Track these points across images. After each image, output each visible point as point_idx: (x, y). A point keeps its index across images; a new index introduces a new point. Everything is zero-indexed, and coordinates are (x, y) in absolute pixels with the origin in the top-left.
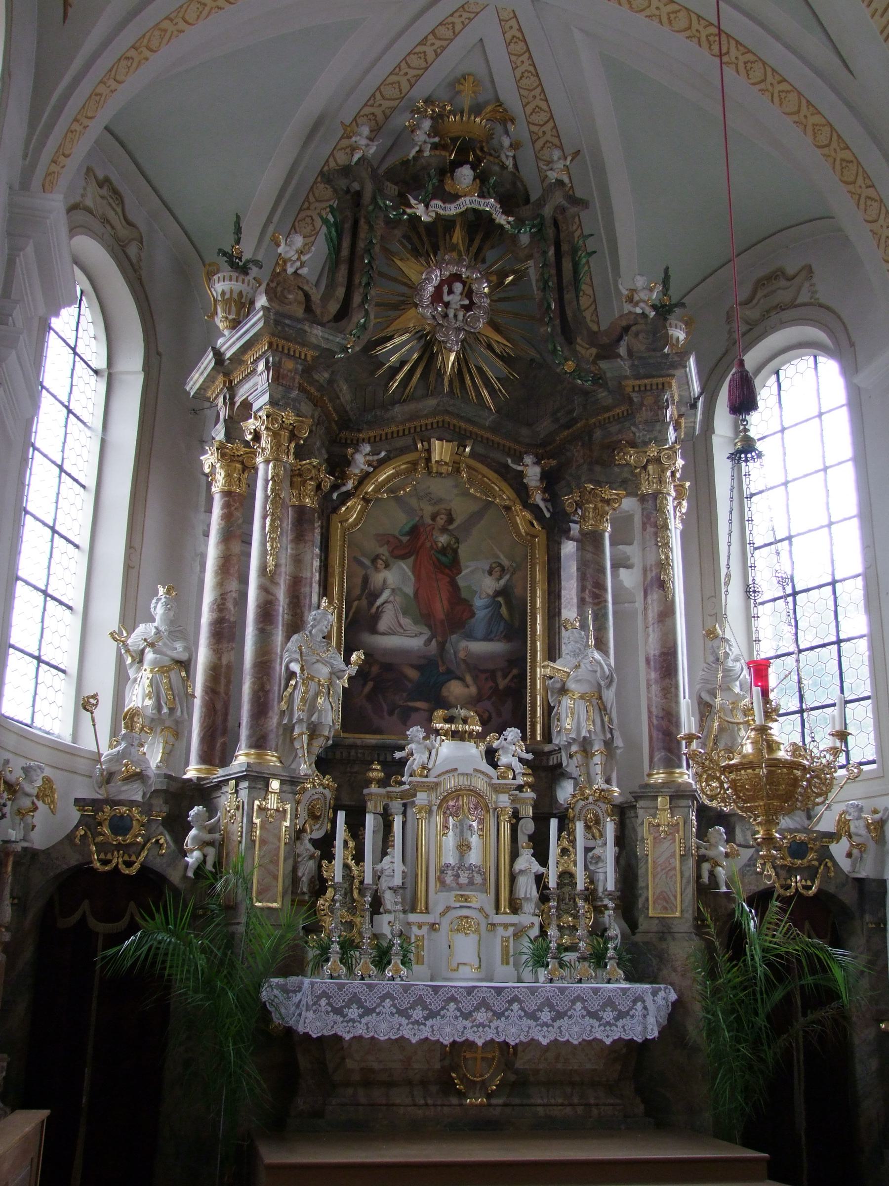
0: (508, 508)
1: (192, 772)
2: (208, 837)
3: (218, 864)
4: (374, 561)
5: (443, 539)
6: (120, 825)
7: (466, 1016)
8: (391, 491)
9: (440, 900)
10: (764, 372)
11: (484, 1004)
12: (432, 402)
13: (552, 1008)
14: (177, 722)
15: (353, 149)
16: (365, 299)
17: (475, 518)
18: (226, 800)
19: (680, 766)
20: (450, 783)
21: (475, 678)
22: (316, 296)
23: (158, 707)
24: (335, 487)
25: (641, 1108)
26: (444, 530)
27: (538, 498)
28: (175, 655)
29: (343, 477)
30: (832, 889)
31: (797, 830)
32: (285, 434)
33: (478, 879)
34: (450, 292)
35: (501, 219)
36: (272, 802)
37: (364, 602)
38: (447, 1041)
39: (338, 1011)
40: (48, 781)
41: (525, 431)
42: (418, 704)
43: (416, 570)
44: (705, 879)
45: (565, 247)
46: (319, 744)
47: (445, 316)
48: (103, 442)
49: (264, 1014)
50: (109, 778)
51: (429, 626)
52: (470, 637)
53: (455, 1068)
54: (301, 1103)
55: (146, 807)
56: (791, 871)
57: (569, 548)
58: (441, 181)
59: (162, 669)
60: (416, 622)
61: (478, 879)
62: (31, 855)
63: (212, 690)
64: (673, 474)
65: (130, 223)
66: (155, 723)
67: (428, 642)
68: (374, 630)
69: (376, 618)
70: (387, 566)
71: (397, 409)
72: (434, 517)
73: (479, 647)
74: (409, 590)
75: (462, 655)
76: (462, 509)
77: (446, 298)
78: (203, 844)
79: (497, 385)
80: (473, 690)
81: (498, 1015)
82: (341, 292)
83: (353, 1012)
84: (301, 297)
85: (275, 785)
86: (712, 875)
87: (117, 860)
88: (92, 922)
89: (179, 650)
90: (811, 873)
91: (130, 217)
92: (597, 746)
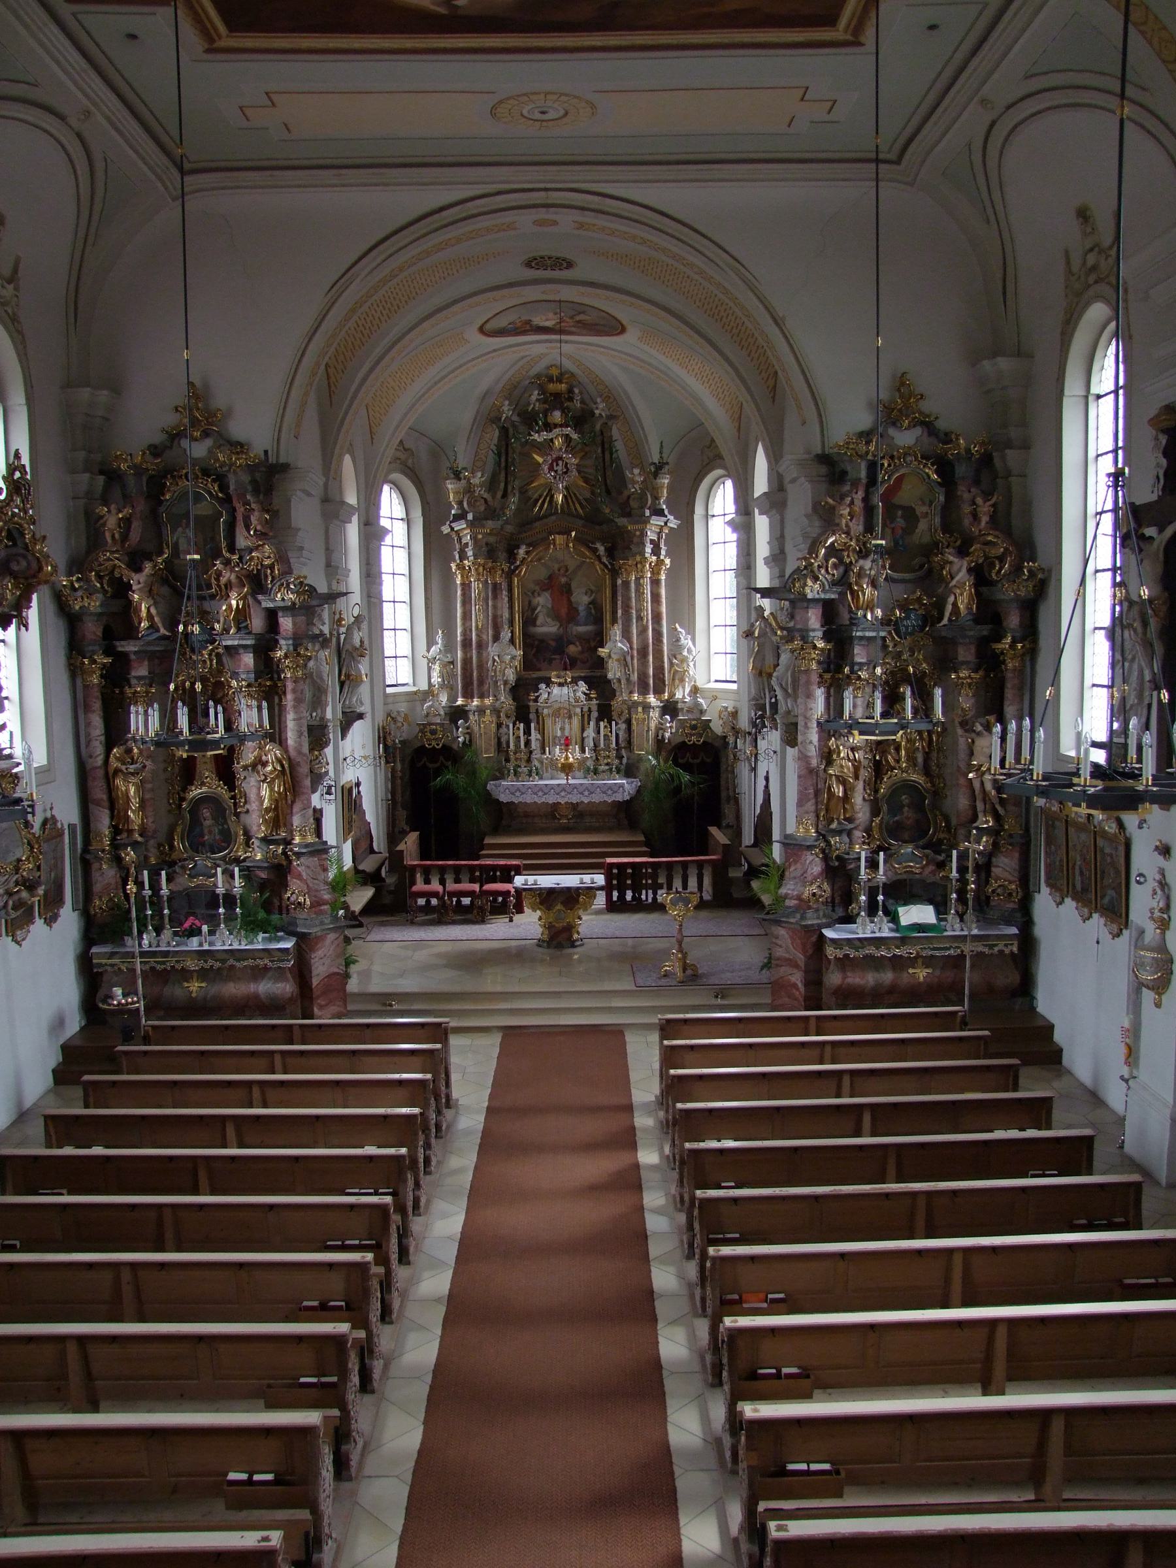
1: (460, 702)
3: (470, 741)
4: (533, 593)
5: (563, 580)
6: (433, 732)
12: (554, 518)
17: (579, 567)
19: (649, 694)
20: (556, 706)
21: (581, 643)
23: (443, 681)
24: (510, 567)
25: (626, 822)
26: (564, 575)
27: (604, 560)
28: (447, 660)
29: (515, 559)
30: (710, 741)
31: (694, 720)
32: (481, 569)
34: (557, 465)
35: (575, 436)
37: (530, 613)
39: (513, 794)
41: (597, 527)
43: (551, 595)
44: (660, 738)
45: (606, 446)
46: (509, 686)
48: (409, 554)
50: (427, 715)
52: (578, 624)
53: (556, 810)
54: (504, 822)
56: (691, 735)
57: (619, 582)
58: (546, 416)
59: (444, 665)
63: (464, 669)
65: (405, 450)
66: (442, 686)
68: (535, 625)
69: (535, 619)
70: (539, 595)
71: (537, 524)
72: (559, 570)
73: (581, 629)
74: (550, 606)
75: (575, 633)
76: (572, 565)
78: (464, 734)
80: (580, 648)
84: (483, 501)
86: (663, 736)
87: (434, 743)
88: (428, 764)
89: (449, 658)
91: (406, 447)
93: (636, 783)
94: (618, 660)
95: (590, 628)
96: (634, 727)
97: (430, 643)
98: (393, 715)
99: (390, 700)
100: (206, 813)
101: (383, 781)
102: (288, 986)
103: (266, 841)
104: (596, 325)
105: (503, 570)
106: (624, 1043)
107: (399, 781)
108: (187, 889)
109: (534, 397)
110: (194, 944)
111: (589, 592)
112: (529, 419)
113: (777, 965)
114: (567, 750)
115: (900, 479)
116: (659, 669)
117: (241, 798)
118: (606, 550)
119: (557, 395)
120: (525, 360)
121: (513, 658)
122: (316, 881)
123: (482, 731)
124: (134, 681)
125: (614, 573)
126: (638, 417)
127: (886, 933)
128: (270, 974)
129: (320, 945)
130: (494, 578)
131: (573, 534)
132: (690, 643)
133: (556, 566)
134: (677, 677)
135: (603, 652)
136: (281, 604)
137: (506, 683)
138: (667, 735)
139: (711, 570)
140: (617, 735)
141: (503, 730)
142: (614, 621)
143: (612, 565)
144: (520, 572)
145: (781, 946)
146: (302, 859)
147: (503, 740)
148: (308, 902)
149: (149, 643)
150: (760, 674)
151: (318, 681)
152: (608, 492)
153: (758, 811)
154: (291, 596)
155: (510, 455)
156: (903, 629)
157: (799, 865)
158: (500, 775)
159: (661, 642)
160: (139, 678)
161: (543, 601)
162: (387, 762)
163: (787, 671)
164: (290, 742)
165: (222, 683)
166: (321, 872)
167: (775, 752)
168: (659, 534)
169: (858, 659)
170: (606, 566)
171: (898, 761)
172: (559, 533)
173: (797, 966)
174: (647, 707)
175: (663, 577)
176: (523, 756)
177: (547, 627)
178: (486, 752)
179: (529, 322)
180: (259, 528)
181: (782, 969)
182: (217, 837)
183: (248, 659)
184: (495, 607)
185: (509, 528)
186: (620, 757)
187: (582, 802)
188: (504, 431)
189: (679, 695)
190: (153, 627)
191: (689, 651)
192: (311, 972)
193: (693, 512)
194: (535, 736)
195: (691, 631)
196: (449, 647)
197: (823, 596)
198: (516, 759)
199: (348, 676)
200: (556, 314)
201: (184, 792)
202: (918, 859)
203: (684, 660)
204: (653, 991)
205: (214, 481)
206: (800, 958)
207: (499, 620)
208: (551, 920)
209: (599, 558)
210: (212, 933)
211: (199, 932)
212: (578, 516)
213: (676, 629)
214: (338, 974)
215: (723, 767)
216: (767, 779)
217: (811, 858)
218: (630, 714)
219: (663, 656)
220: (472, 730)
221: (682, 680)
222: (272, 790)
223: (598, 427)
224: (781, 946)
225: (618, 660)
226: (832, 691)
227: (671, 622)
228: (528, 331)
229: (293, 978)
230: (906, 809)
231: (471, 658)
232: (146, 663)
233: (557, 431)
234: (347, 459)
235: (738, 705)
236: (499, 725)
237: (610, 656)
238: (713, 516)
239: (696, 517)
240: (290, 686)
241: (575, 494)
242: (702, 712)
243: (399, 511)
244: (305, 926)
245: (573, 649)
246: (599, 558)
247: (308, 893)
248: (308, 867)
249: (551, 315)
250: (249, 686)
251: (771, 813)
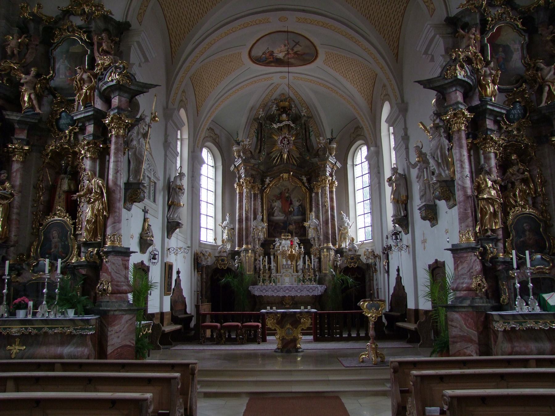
0: (301, 187)
1: (236, 249)
2: (239, 261)
4: (273, 201)
5: (287, 195)
6: (223, 260)
7: (285, 291)
8: (276, 185)
9: (282, 271)
10: (358, 149)
11: (288, 289)
12: (282, 165)
13: (300, 289)
14: (233, 240)
15: (260, 114)
16: (264, 148)
18: (242, 255)
21: (295, 224)
22: (253, 151)
23: (229, 237)
24: (262, 187)
26: (287, 193)
27: (306, 184)
29: (265, 184)
30: (360, 266)
32: (248, 182)
33: (290, 267)
34: (284, 141)
35: (292, 125)
36: (249, 255)
37: (271, 210)
38: (281, 296)
39: (261, 291)
40: (210, 253)
42: (283, 231)
44: (335, 265)
45: (307, 129)
46: (261, 242)
47: (283, 146)
49: (249, 292)
50: (220, 252)
51: (285, 214)
52: (294, 215)
55: (227, 257)
56: (351, 263)
57: (313, 195)
58: (279, 118)
59: (229, 230)
60: (282, 213)
61: (290, 267)
62: (208, 267)
63: (239, 233)
64: (329, 181)
65: (215, 134)
66: (228, 240)
67: (285, 217)
68: (273, 216)
69: (274, 213)
70: (275, 202)
72: (285, 190)
74: (280, 207)
77: (283, 142)
79: (297, 159)
80: (295, 227)
81: (290, 291)
82: (259, 147)
83: (264, 291)
85: (250, 251)
86: (337, 264)
87: (223, 266)
89: (232, 226)
90: (355, 263)
91: (216, 133)
92: (316, 239)
93: (324, 287)
94: (313, 229)
95: (300, 217)
96: (322, 259)
97: (224, 219)
98: (203, 253)
99: (202, 246)
100: (55, 234)
101: (196, 281)
102: (86, 350)
103: (87, 244)
104: (304, 54)
105: (259, 188)
106: (342, 404)
107: (204, 284)
108: (30, 281)
109: (274, 108)
110: (21, 314)
111: (299, 200)
112: (271, 119)
113: (454, 342)
114: (291, 248)
115: (499, 29)
116: (334, 233)
117: (79, 224)
118: (307, 179)
119: (284, 108)
120: (271, 88)
121: (263, 228)
122: (118, 275)
123: (247, 261)
124: (15, 141)
125: (311, 190)
126: (321, 120)
127: (538, 310)
128: (75, 341)
129: (116, 322)
130: (255, 191)
131: (292, 173)
132: (348, 220)
133: (284, 188)
134: (342, 237)
135: (306, 224)
136: (111, 84)
137: (259, 240)
138: (338, 263)
139: (356, 189)
140: (314, 265)
141: (257, 262)
142: (311, 210)
143: (310, 187)
144: (267, 191)
145: (456, 327)
146: (109, 257)
147: (257, 267)
148: (110, 288)
149: (27, 116)
150: (398, 202)
151: (139, 156)
152: (308, 150)
153: (392, 291)
154: (117, 77)
155: (263, 134)
156: (511, 116)
157: (465, 265)
158: (255, 283)
159: (334, 220)
160: (17, 139)
161: (277, 204)
162: (198, 271)
163: (437, 149)
164: (111, 177)
165: (76, 152)
166: (123, 269)
167: (407, 246)
168: (332, 169)
169: (489, 127)
170: (307, 188)
171: (516, 202)
172: (285, 173)
173: (471, 341)
174: (329, 249)
175: (334, 190)
176: (267, 276)
177: (279, 217)
178: (249, 272)
179: (272, 53)
180: (105, 48)
181: (458, 345)
182: (60, 250)
183: (90, 129)
184: (255, 204)
185: (262, 168)
186: (316, 276)
187: (297, 296)
188: (260, 125)
189: (343, 245)
190: (32, 107)
191: (348, 224)
192: (107, 341)
193: (347, 163)
194: (273, 264)
195: (348, 215)
196: (232, 221)
197: (466, 79)
198: (264, 276)
199: (172, 202)
200: (285, 46)
201: (43, 220)
202: (546, 263)
203: (346, 228)
204: (357, 370)
205: (84, 32)
206: (474, 334)
207: (257, 210)
208: (284, 334)
209: (303, 183)
210: (36, 307)
211: (25, 307)
212: (294, 165)
213: (342, 214)
214: (130, 346)
215: (367, 280)
216: (398, 270)
217: (474, 258)
218: (320, 254)
219: (335, 227)
220: (242, 261)
221: (345, 239)
222: (93, 209)
223: (303, 121)
224: (456, 327)
225: (313, 229)
226: (472, 152)
227: (339, 214)
228: (271, 62)
229: (94, 346)
230: (527, 233)
231: (243, 228)
232: (26, 132)
233: (284, 123)
234: (182, 112)
235: (374, 248)
236: (255, 260)
237: (309, 227)
238: (356, 165)
239: (348, 166)
240: (113, 140)
241: (293, 156)
242: (355, 251)
243: (211, 162)
244: (106, 306)
245: (291, 227)
246: (303, 183)
247: (111, 282)
248: (114, 264)
249: (283, 48)
250: (88, 144)
251: (404, 287)
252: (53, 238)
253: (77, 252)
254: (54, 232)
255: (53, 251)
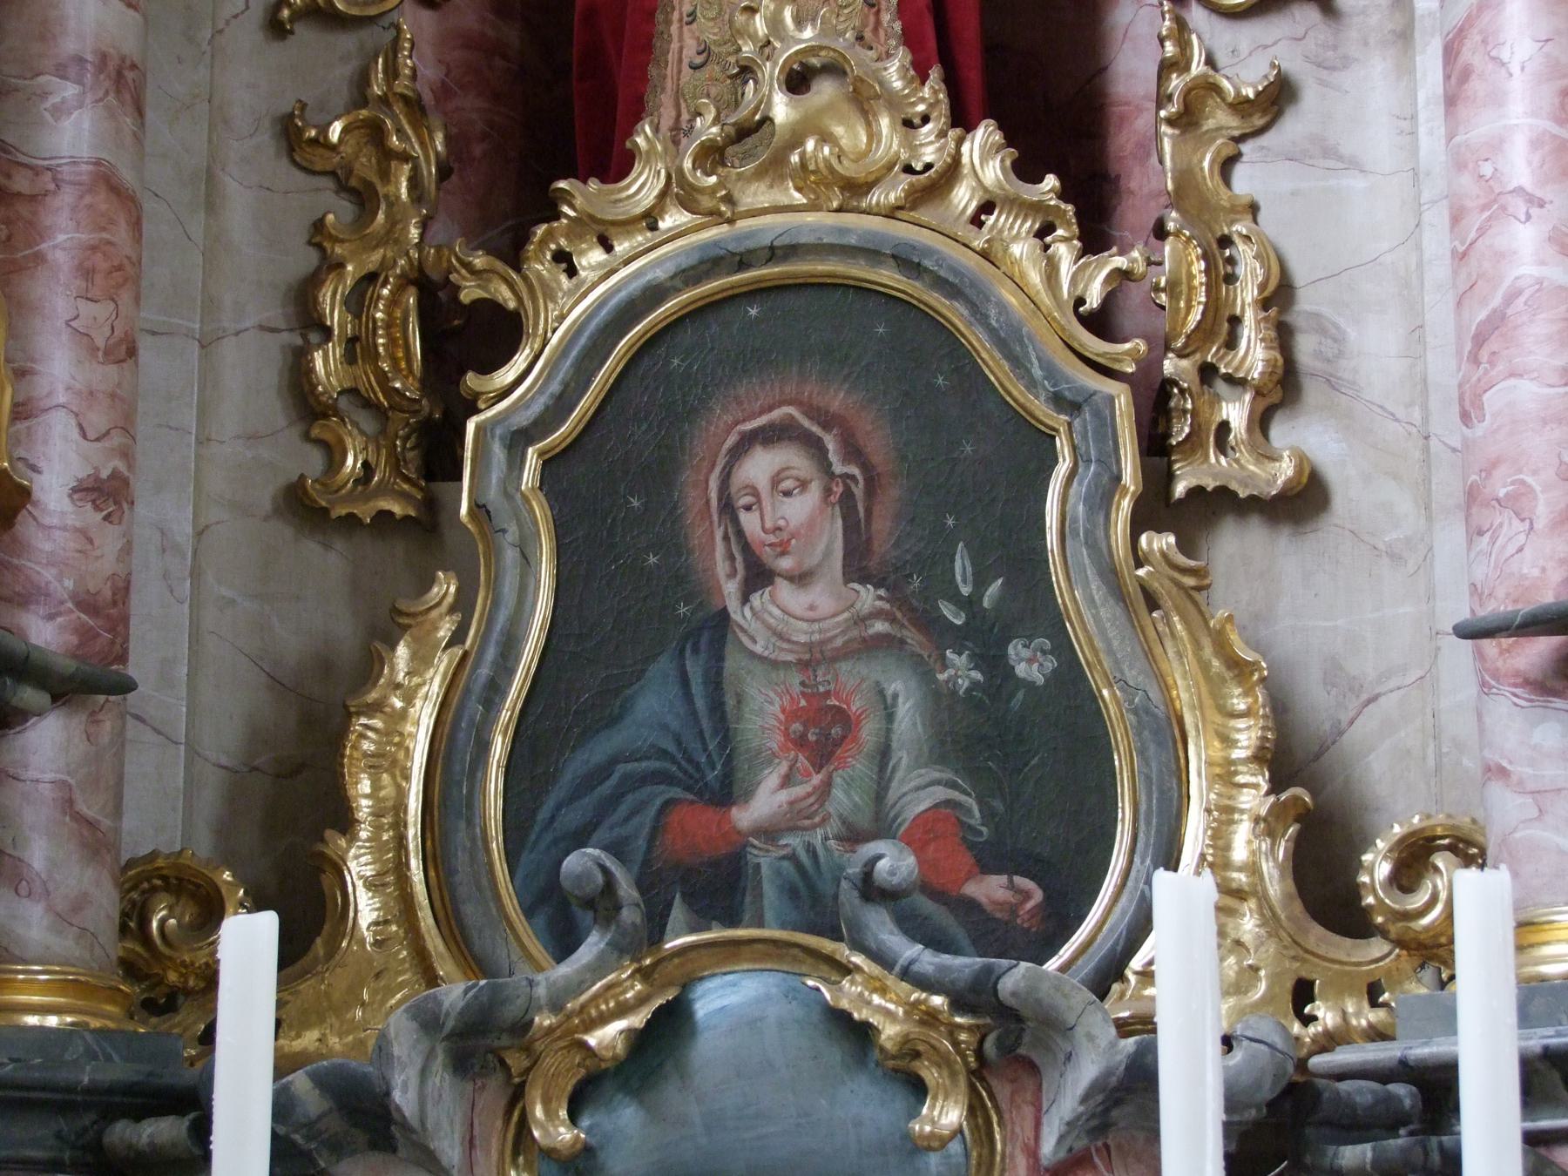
252: (758, 576)
253: (1268, 826)
254: (759, 467)
255: (793, 820)
